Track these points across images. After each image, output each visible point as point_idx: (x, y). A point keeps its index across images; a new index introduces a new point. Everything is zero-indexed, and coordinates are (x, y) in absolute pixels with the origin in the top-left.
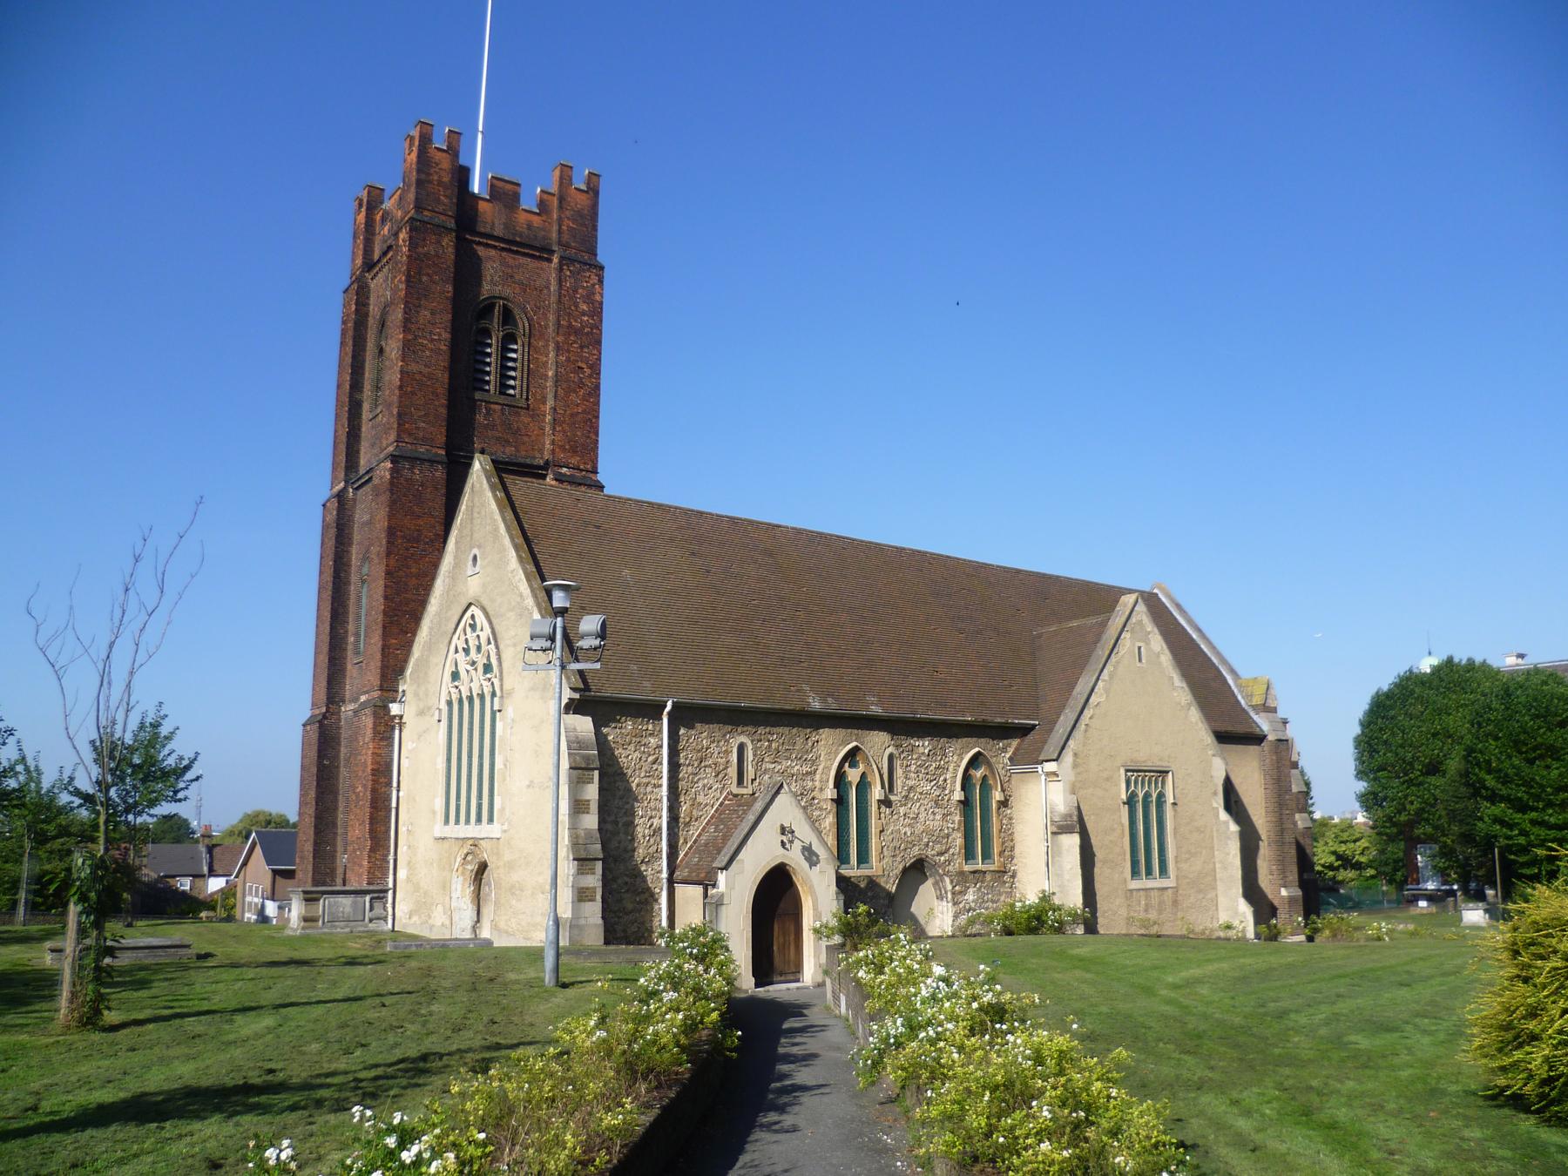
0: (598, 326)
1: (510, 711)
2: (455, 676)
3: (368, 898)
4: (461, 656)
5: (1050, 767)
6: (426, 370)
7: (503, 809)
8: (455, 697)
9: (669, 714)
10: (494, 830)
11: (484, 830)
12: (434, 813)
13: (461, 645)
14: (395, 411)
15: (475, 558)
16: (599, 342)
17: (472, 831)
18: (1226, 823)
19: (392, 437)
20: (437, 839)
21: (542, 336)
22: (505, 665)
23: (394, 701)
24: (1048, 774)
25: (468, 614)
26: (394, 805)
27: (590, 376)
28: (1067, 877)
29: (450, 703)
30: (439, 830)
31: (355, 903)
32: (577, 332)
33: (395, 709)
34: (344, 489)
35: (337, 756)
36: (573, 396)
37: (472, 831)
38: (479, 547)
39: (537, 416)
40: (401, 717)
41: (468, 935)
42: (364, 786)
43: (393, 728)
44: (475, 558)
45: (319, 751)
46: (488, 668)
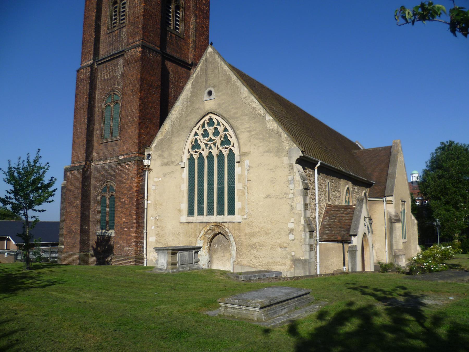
0: (208, 11)
1: (247, 163)
2: (196, 146)
3: (193, 252)
4: (200, 137)
5: (388, 198)
6: (153, 11)
7: (243, 209)
8: (196, 156)
9: (318, 167)
10: (237, 218)
11: (226, 218)
12: (180, 210)
13: (200, 132)
14: (140, 26)
15: (210, 93)
16: (208, 18)
17: (215, 218)
18: (414, 220)
19: (138, 37)
20: (181, 223)
21: (188, 10)
22: (241, 141)
23: (144, 159)
24: (387, 201)
25: (207, 117)
26: (146, 207)
27: (206, 31)
28: (398, 238)
29: (191, 159)
30: (185, 217)
31: (189, 254)
32: (202, 11)
33: (146, 162)
34: (93, 64)
35: (89, 186)
36: (201, 38)
37: (215, 218)
38: (214, 87)
39: (187, 44)
40: (149, 166)
41: (206, 267)
42: (131, 199)
43: (145, 171)
44: (210, 93)
45: (83, 183)
46: (226, 141)
